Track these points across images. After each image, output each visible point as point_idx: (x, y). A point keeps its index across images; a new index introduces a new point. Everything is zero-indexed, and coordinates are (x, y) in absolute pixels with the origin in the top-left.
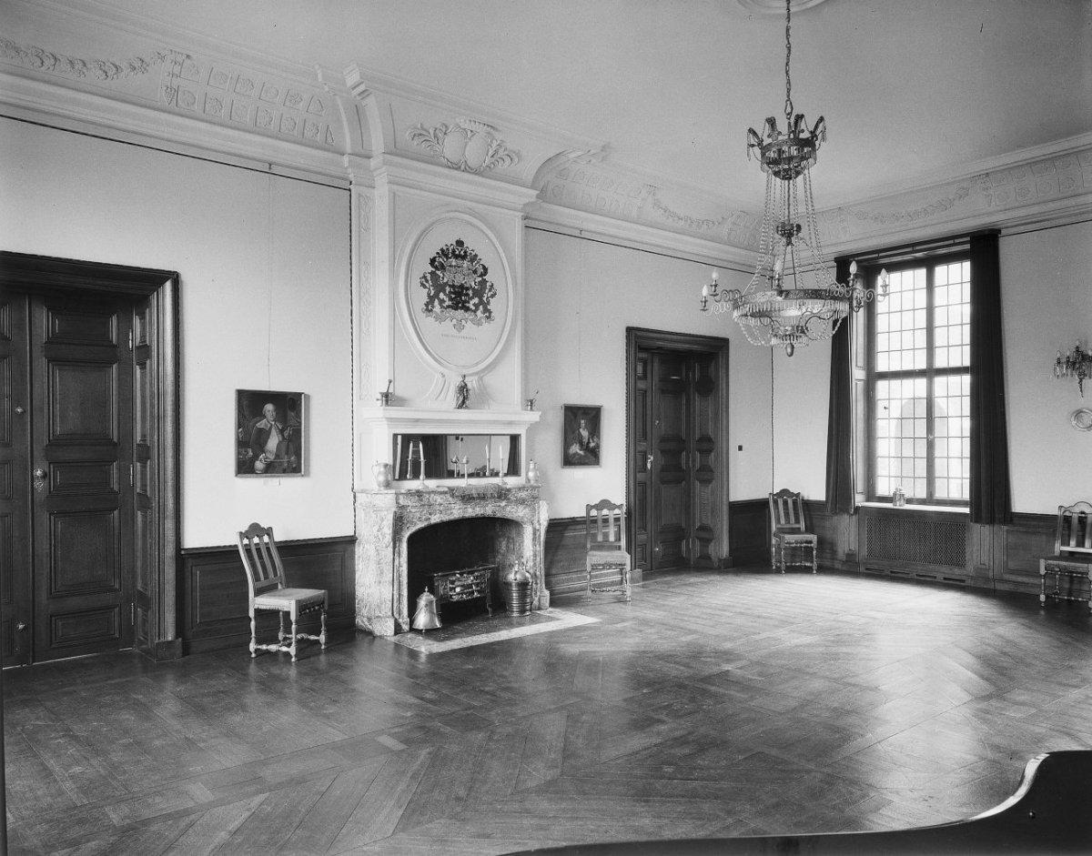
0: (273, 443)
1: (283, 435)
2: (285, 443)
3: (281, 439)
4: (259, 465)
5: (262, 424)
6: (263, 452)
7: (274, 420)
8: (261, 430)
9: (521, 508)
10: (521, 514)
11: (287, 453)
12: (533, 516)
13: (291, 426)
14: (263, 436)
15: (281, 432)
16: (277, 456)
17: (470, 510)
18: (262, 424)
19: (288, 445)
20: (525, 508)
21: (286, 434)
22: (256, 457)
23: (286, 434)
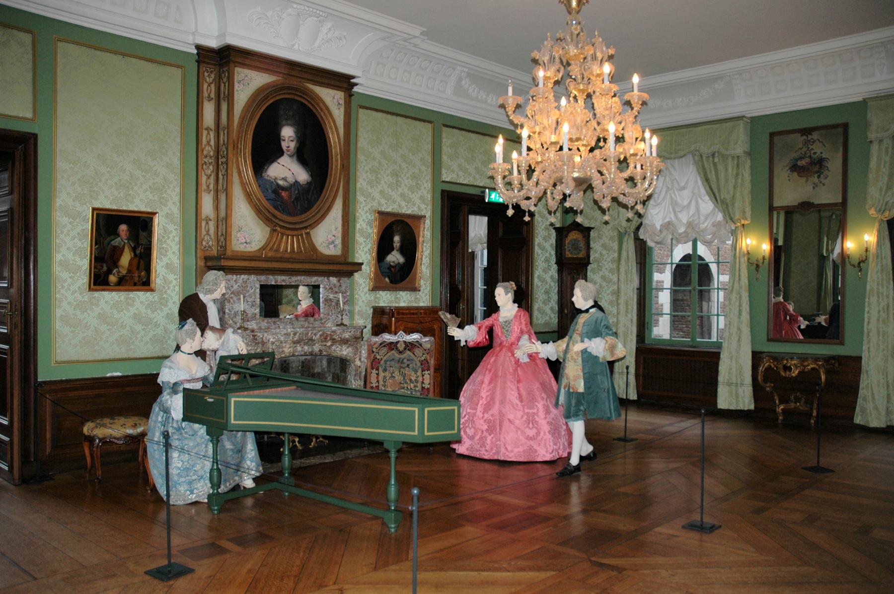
0: (126, 259)
1: (135, 253)
2: (137, 259)
3: (133, 256)
4: (113, 278)
5: (116, 242)
6: (117, 267)
7: (128, 239)
8: (115, 248)
9: (344, 347)
10: (345, 353)
11: (138, 268)
12: (355, 354)
13: (142, 244)
14: (116, 253)
15: (134, 249)
16: (129, 271)
17: (299, 348)
18: (116, 242)
19: (139, 262)
20: (348, 347)
21: (138, 252)
22: (109, 272)
23: (138, 252)
